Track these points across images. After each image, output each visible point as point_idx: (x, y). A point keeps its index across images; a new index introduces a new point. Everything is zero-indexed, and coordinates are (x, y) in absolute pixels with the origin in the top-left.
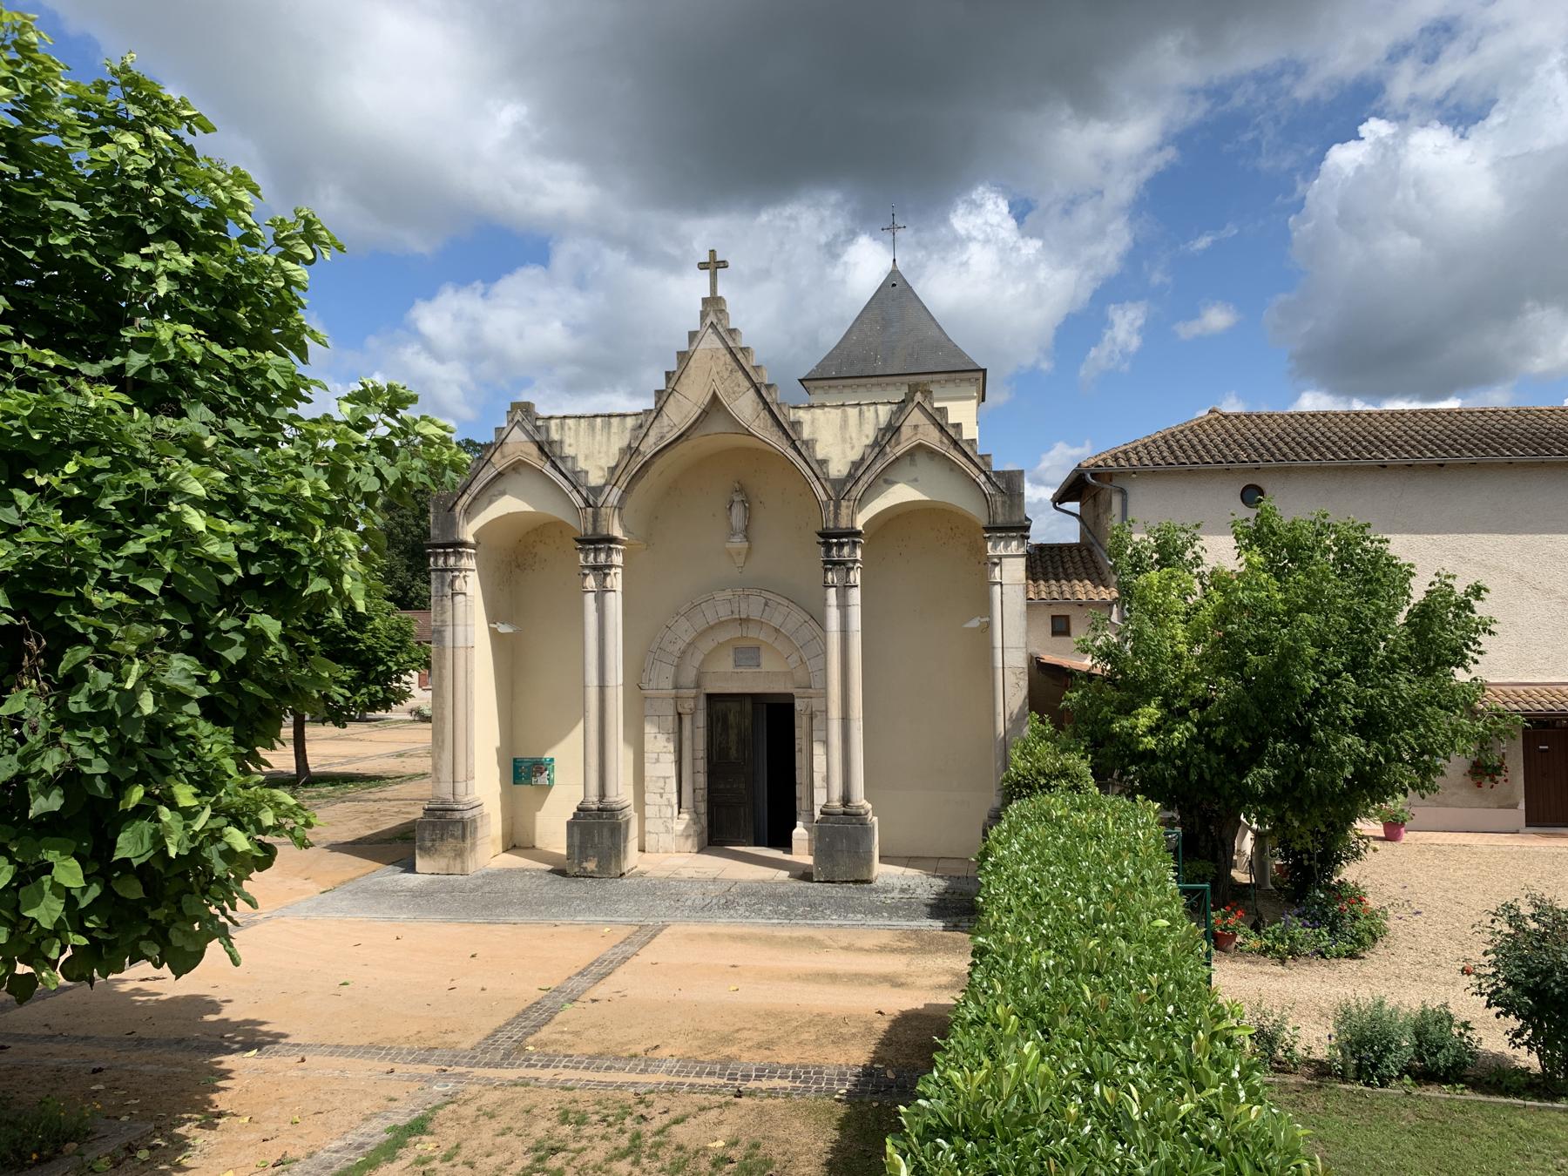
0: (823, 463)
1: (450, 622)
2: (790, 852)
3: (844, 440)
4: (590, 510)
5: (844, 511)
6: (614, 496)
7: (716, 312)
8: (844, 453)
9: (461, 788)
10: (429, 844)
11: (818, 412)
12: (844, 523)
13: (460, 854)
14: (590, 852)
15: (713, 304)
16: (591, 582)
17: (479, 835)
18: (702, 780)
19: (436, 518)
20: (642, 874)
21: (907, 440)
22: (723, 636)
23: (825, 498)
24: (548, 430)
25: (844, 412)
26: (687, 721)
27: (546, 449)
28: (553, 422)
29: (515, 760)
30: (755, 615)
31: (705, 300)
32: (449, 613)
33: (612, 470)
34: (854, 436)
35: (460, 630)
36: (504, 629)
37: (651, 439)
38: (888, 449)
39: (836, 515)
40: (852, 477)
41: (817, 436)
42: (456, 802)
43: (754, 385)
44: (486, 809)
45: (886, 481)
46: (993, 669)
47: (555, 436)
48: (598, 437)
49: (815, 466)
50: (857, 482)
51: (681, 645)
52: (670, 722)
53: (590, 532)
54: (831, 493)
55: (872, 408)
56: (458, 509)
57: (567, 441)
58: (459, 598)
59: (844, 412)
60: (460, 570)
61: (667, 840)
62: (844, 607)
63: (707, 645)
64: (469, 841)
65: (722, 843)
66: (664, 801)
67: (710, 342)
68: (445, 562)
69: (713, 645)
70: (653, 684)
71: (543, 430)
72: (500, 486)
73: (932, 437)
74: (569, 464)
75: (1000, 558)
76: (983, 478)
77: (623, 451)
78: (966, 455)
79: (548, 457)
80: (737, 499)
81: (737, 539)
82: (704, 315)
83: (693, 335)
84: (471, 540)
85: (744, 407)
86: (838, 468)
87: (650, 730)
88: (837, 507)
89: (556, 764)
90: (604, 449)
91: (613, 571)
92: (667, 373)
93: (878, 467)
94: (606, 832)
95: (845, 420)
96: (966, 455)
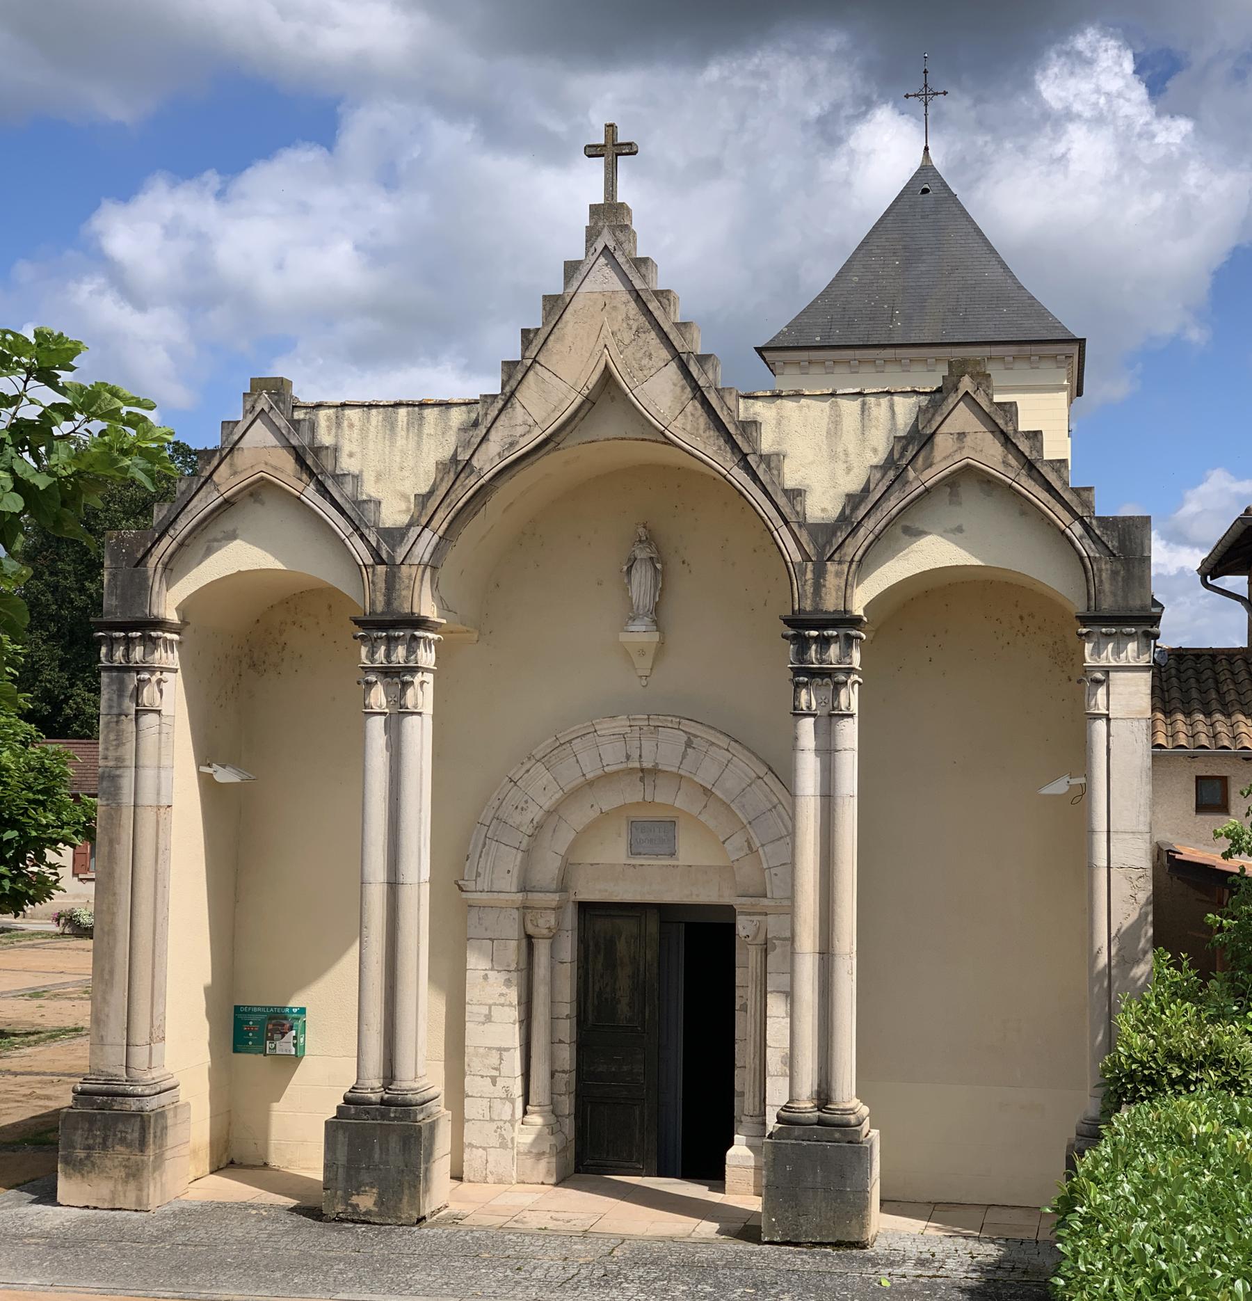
0: (796, 494)
2: (721, 1188)
3: (833, 456)
4: (381, 569)
5: (832, 581)
6: (425, 545)
7: (613, 229)
8: (833, 476)
9: (140, 1056)
10: (81, 1154)
11: (789, 404)
12: (831, 603)
13: (134, 1173)
14: (365, 1177)
15: (609, 216)
16: (378, 697)
17: (170, 1140)
18: (566, 1056)
19: (114, 576)
20: (456, 1219)
21: (945, 457)
22: (610, 800)
23: (797, 557)
24: (313, 427)
25: (835, 406)
27: (310, 461)
28: (323, 414)
29: (237, 1008)
30: (669, 762)
31: (594, 210)
32: (130, 746)
33: (423, 499)
34: (851, 449)
35: (148, 775)
36: (224, 776)
37: (494, 446)
38: (911, 474)
39: (818, 587)
40: (847, 521)
41: (785, 448)
42: (132, 1081)
43: (677, 356)
44: (183, 1095)
46: (1091, 868)
47: (325, 438)
48: (400, 442)
49: (781, 501)
50: (854, 531)
51: (535, 813)
52: (512, 951)
53: (380, 607)
54: (810, 549)
56: (152, 561)
57: (346, 447)
58: (149, 720)
59: (835, 406)
60: (152, 670)
61: (502, 1162)
62: (827, 751)
63: (580, 816)
64: (151, 1151)
66: (498, 1091)
67: (602, 280)
68: (127, 655)
69: (593, 814)
70: (483, 883)
71: (305, 427)
72: (227, 524)
73: (988, 454)
74: (348, 488)
75: (1107, 671)
76: (1078, 528)
78: (1049, 488)
79: (312, 475)
80: (642, 554)
81: (639, 626)
82: (592, 234)
83: (571, 269)
84: (172, 616)
85: (659, 394)
86: (822, 505)
88: (820, 573)
89: (309, 1017)
90: (410, 462)
91: (418, 678)
92: (525, 332)
93: (893, 504)
94: (394, 1143)
96: (1049, 488)
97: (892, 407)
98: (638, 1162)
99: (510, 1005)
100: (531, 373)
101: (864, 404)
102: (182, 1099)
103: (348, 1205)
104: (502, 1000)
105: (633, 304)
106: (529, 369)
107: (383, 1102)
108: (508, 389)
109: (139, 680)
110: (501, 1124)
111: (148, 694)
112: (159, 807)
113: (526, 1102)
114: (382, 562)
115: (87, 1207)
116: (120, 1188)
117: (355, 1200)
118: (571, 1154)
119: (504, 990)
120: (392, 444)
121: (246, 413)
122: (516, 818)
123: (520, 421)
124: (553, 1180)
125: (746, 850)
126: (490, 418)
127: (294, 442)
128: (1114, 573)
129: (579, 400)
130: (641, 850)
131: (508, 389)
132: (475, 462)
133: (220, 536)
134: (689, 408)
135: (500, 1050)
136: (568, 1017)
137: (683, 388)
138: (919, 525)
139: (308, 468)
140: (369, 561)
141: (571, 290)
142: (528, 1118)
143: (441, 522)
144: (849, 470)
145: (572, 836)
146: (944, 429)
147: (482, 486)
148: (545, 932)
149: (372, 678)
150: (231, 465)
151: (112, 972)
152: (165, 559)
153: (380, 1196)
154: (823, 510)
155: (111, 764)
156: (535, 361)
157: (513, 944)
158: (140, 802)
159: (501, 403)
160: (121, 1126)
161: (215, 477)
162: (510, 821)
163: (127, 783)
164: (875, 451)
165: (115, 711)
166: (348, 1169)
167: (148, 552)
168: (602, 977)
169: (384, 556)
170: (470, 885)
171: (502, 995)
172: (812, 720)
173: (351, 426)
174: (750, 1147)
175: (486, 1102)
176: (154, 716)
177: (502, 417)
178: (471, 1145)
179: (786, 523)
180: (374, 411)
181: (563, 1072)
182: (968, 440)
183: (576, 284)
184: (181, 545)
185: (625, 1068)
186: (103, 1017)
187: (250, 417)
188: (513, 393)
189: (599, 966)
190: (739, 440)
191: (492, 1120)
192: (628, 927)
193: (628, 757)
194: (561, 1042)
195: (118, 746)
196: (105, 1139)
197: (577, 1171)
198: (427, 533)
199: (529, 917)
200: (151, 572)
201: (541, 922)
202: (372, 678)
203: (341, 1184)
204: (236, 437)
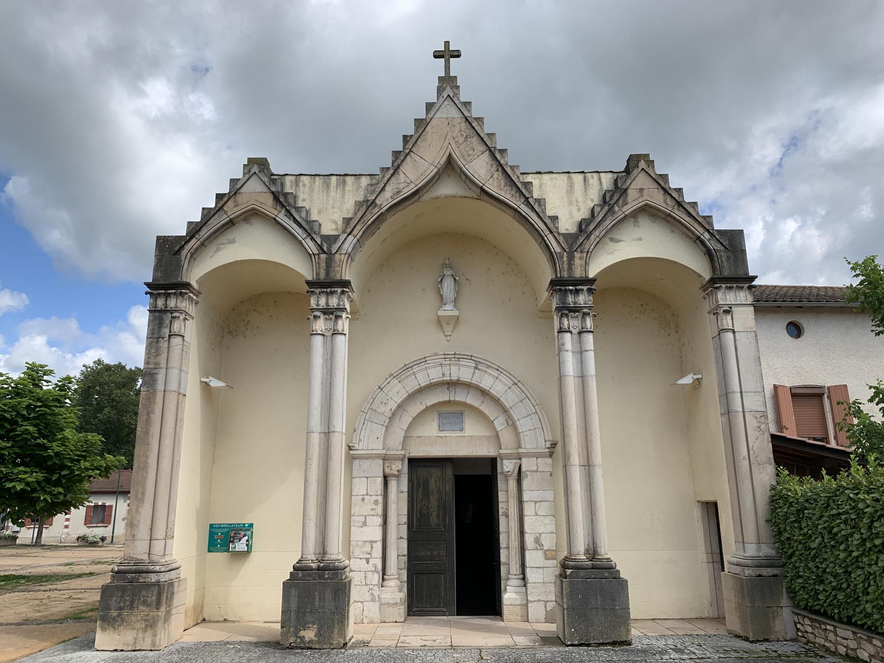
0: (555, 219)
1: (163, 365)
3: (570, 203)
4: (323, 256)
5: (578, 262)
6: (348, 245)
7: (452, 88)
8: (571, 213)
9: (158, 547)
10: (114, 613)
11: (546, 177)
12: (578, 273)
13: (151, 625)
14: (309, 618)
15: (447, 82)
16: (320, 325)
18: (404, 544)
20: (365, 644)
21: (633, 201)
23: (558, 250)
24: (282, 185)
25: (570, 178)
27: (282, 199)
28: (288, 178)
29: (211, 526)
31: (441, 79)
33: (347, 221)
34: (580, 199)
35: (174, 373)
38: (616, 208)
42: (154, 563)
43: (489, 149)
45: (612, 240)
47: (288, 189)
48: (332, 194)
49: (548, 221)
50: (588, 237)
53: (322, 276)
54: (565, 246)
55: (595, 175)
56: (184, 252)
57: (301, 196)
58: (176, 341)
62: (581, 352)
63: (416, 408)
64: (163, 609)
66: (370, 567)
67: (448, 112)
69: (423, 407)
71: (279, 182)
72: (229, 235)
73: (657, 199)
74: (304, 214)
76: (707, 235)
77: (359, 204)
78: (689, 214)
79: (283, 206)
80: (448, 272)
82: (440, 90)
83: (429, 106)
86: (567, 225)
87: (360, 487)
88: (571, 258)
89: (255, 529)
92: (405, 137)
94: (328, 595)
95: (571, 186)
96: (689, 214)
97: (600, 179)
99: (377, 515)
100: (408, 158)
101: (585, 178)
102: (182, 577)
103: (297, 637)
104: (373, 512)
105: (463, 124)
106: (407, 154)
107: (319, 569)
108: (396, 164)
109: (173, 318)
110: (371, 587)
111: (177, 326)
112: (179, 394)
113: (384, 574)
114: (324, 252)
115: (116, 650)
116: (140, 635)
117: (302, 633)
119: (374, 506)
120: (328, 195)
121: (244, 174)
122: (382, 409)
123: (402, 181)
124: (402, 620)
125: (506, 425)
126: (386, 179)
127: (273, 189)
128: (728, 258)
129: (435, 170)
131: (396, 164)
132: (377, 202)
133: (225, 241)
134: (496, 175)
135: (371, 542)
137: (492, 165)
138: (618, 237)
139: (281, 203)
140: (316, 252)
141: (430, 116)
142: (385, 583)
143: (359, 231)
144: (579, 210)
145: (410, 419)
146: (632, 186)
147: (382, 213)
148: (396, 473)
149: (318, 313)
150: (235, 201)
151: (143, 494)
152: (193, 251)
153: (319, 630)
154: (567, 229)
155: (152, 366)
156: (410, 151)
158: (168, 388)
159: (392, 171)
160: (144, 593)
161: (225, 208)
162: (378, 411)
163: (161, 378)
164: (592, 200)
165: (156, 336)
166: (298, 613)
167: (182, 247)
169: (325, 249)
170: (357, 446)
171: (372, 509)
172: (569, 334)
173: (304, 185)
175: (363, 574)
176: (179, 339)
177: (393, 179)
179: (551, 232)
180: (317, 178)
182: (645, 192)
183: (433, 113)
184: (202, 244)
186: (136, 522)
187: (247, 176)
188: (398, 167)
189: (420, 496)
190: (524, 191)
191: (366, 585)
192: (436, 472)
193: (443, 375)
194: (401, 538)
195: (156, 356)
196: (132, 602)
197: (409, 615)
198: (351, 238)
199: (386, 465)
200: (183, 258)
201: (394, 467)
202: (318, 313)
203: (293, 623)
204: (239, 186)
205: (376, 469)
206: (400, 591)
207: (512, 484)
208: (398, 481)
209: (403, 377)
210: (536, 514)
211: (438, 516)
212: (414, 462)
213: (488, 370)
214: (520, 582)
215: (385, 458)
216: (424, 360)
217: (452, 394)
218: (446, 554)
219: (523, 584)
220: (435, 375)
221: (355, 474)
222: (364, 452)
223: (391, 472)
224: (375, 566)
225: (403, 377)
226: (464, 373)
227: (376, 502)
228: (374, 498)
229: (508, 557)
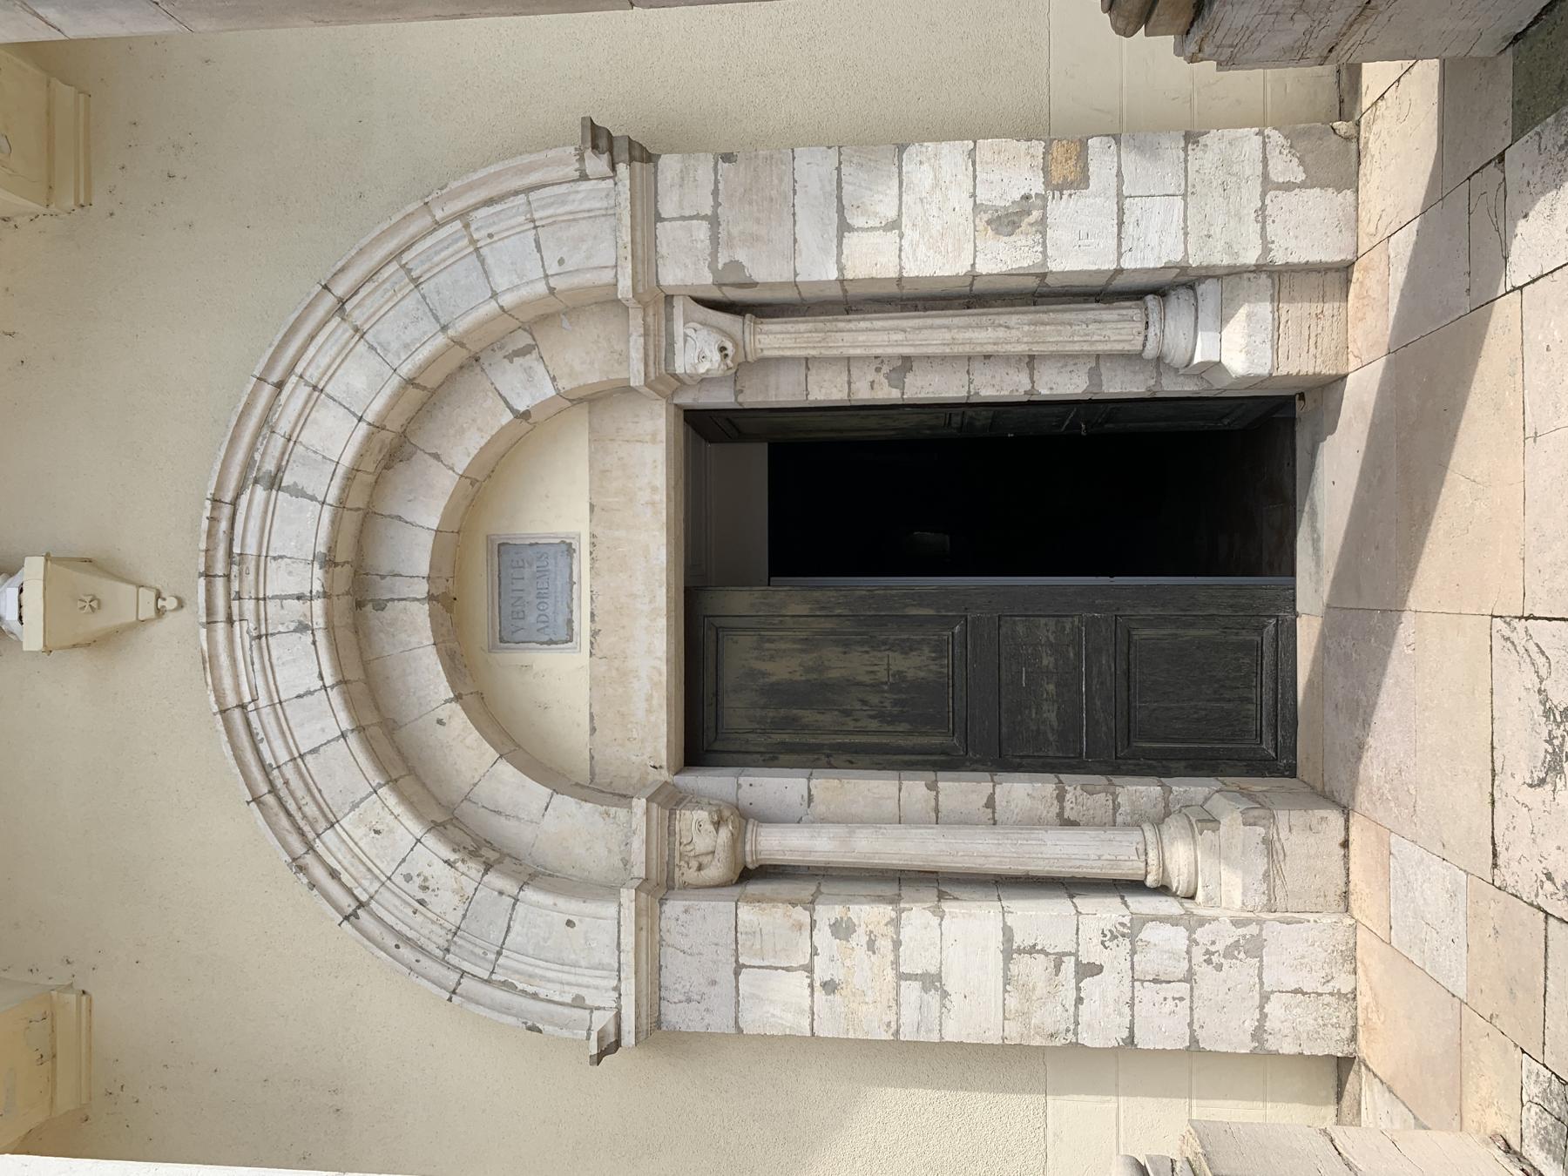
2: (1325, 391)
18: (1022, 792)
22: (424, 677)
26: (775, 843)
51: (432, 857)
52: (765, 918)
61: (1298, 950)
63: (462, 749)
65: (1285, 717)
66: (1114, 958)
69: (458, 719)
87: (780, 1003)
98: (1260, 629)
99: (896, 923)
104: (885, 945)
110: (1198, 953)
113: (1136, 886)
118: (1257, 785)
119: (860, 938)
122: (446, 903)
124: (1335, 818)
125: (531, 360)
130: (561, 619)
135: (1010, 951)
136: (932, 787)
142: (1178, 882)
145: (507, 770)
148: (725, 834)
157: (747, 913)
162: (454, 918)
168: (847, 713)
170: (602, 1020)
171: (871, 946)
174: (1222, 320)
175: (1146, 993)
178: (1259, 1033)
181: (1061, 798)
185: (1047, 661)
189: (827, 719)
191: (1189, 977)
192: (740, 657)
193: (302, 628)
194: (990, 803)
197: (1291, 771)
199: (691, 875)
201: (702, 843)
205: (700, 923)
206: (1212, 821)
207: (774, 338)
208: (766, 819)
209: (311, 810)
210: (894, 225)
211: (907, 648)
212: (700, 743)
213: (284, 426)
214: (1179, 305)
215: (662, 884)
216: (236, 717)
217: (402, 588)
218: (1050, 616)
219: (1184, 294)
220: (302, 665)
221: (720, 1022)
222: (629, 987)
223: (722, 854)
224: (1109, 937)
225: (311, 810)
226: (293, 537)
227: (842, 930)
228: (823, 936)
229: (1066, 359)
